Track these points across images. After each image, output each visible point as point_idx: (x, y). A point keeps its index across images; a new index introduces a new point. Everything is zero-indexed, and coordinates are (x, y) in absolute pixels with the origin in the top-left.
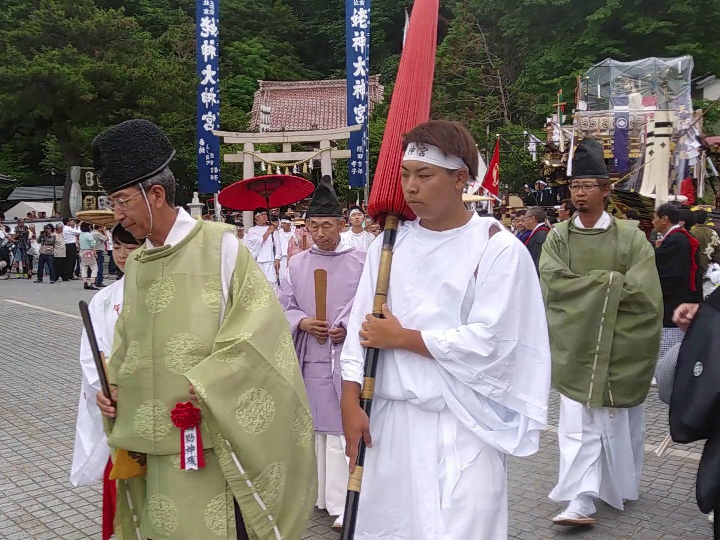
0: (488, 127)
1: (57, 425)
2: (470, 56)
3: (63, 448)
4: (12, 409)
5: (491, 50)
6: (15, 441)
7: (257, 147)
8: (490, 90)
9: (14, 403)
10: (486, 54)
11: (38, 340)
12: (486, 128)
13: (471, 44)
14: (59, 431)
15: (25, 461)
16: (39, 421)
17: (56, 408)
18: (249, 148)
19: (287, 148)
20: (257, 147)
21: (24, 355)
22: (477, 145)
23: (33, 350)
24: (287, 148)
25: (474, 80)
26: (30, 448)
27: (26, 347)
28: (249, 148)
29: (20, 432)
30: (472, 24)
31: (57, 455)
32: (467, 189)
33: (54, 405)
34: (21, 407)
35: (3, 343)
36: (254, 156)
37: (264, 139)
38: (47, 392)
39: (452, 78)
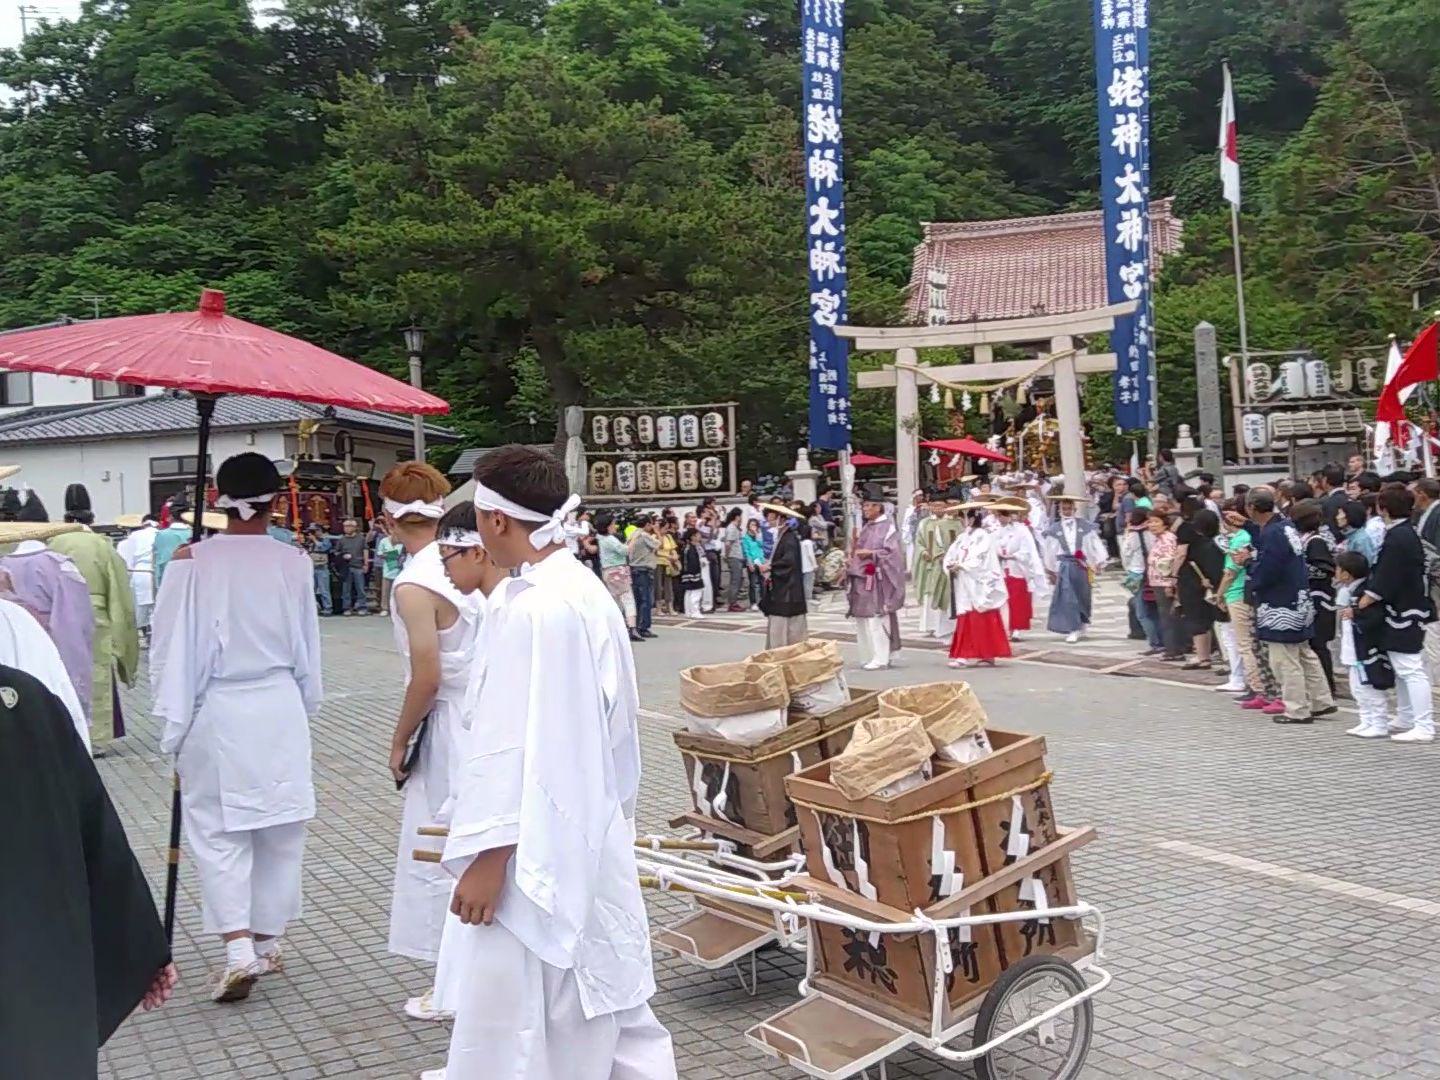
0: (1416, 296)
2: (1368, 153)
5: (1413, 136)
7: (921, 354)
8: (1416, 217)
10: (1404, 145)
12: (1410, 299)
13: (1367, 125)
18: (906, 357)
19: (984, 355)
20: (921, 354)
22: (1392, 336)
24: (984, 355)
25: (1378, 202)
28: (906, 357)
30: (1370, 85)
32: (1374, 426)
36: (915, 372)
37: (935, 337)
39: (1328, 199)
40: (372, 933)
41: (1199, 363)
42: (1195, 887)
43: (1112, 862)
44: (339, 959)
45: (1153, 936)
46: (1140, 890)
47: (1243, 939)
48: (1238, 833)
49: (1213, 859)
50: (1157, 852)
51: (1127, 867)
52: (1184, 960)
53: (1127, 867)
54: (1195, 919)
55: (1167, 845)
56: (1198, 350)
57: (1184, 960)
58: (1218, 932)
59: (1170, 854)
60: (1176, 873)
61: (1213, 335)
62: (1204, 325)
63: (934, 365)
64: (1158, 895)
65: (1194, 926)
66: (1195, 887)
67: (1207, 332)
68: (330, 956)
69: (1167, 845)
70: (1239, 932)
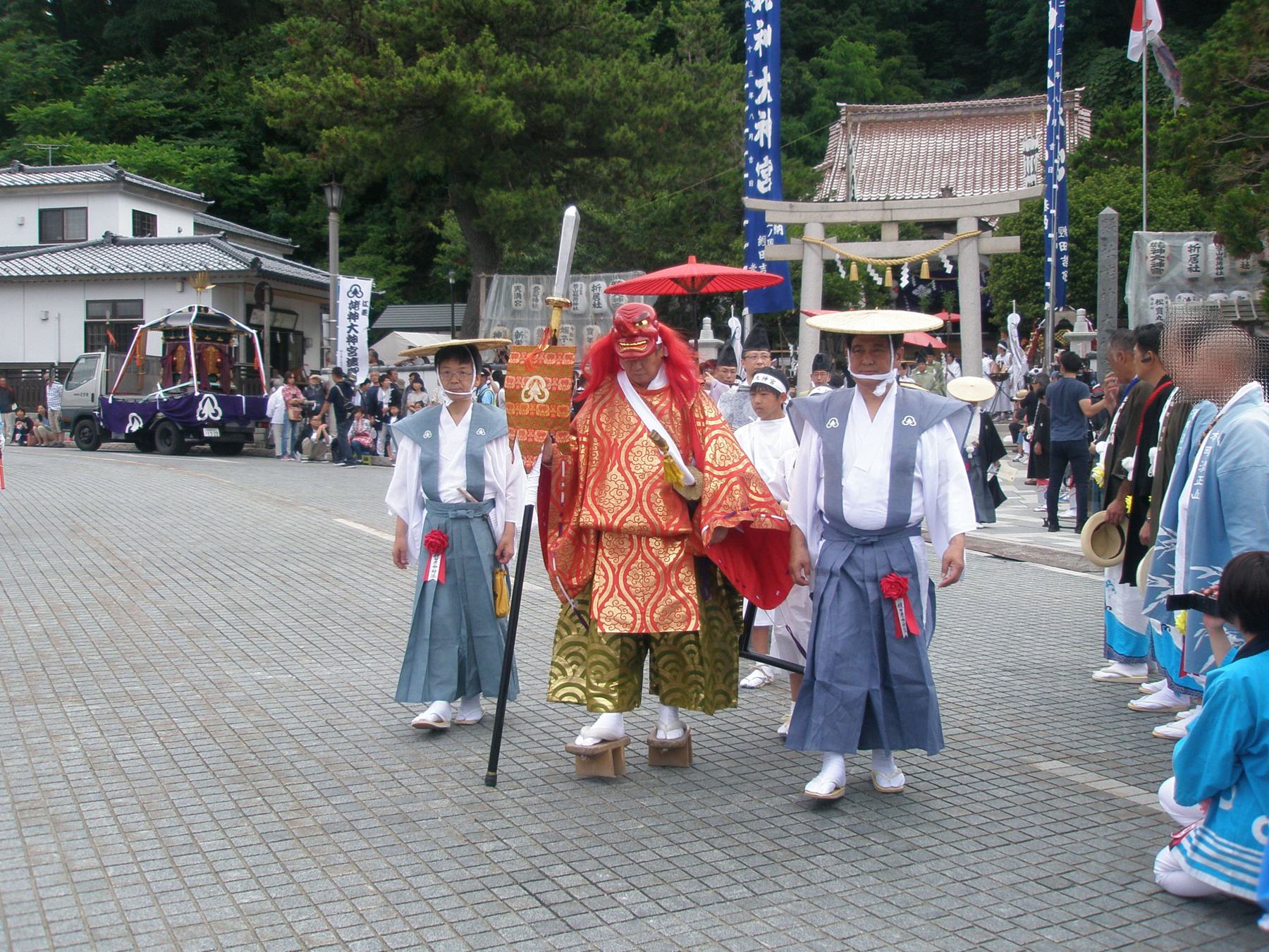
1: (357, 815)
3: (353, 878)
4: (279, 767)
6: (263, 849)
9: (287, 753)
11: (370, 608)
14: (358, 831)
15: (268, 905)
16: (323, 802)
17: (366, 771)
18: (814, 232)
19: (890, 233)
21: (335, 641)
23: (357, 630)
24: (890, 233)
26: (286, 871)
27: (343, 622)
28: (814, 232)
29: (278, 826)
31: (337, 895)
33: (365, 764)
34: (298, 765)
35: (305, 610)
36: (822, 247)
37: (843, 215)
38: (358, 732)
40: (152, 834)
41: (1100, 247)
42: (1077, 822)
43: (985, 786)
44: (104, 867)
45: (1024, 887)
46: (1015, 823)
47: (1129, 896)
48: (1124, 753)
49: (1100, 786)
50: (1034, 775)
51: (1001, 793)
52: (1062, 924)
53: (1001, 793)
54: (1074, 868)
55: (1045, 766)
56: (1101, 234)
57: (1062, 924)
58: (1104, 887)
59: (1053, 778)
60: (1056, 803)
61: (1116, 220)
62: (1108, 211)
63: (840, 241)
64: (1034, 832)
65: (1073, 876)
66: (1077, 822)
67: (1111, 218)
68: (95, 862)
69: (1045, 766)
70: (1125, 887)
